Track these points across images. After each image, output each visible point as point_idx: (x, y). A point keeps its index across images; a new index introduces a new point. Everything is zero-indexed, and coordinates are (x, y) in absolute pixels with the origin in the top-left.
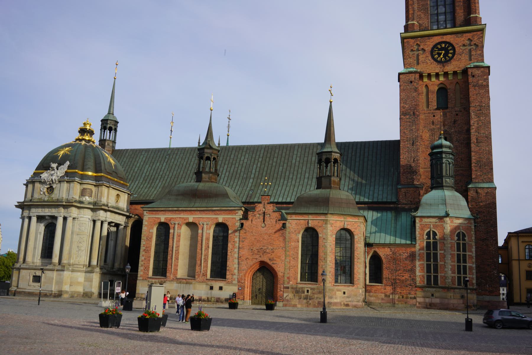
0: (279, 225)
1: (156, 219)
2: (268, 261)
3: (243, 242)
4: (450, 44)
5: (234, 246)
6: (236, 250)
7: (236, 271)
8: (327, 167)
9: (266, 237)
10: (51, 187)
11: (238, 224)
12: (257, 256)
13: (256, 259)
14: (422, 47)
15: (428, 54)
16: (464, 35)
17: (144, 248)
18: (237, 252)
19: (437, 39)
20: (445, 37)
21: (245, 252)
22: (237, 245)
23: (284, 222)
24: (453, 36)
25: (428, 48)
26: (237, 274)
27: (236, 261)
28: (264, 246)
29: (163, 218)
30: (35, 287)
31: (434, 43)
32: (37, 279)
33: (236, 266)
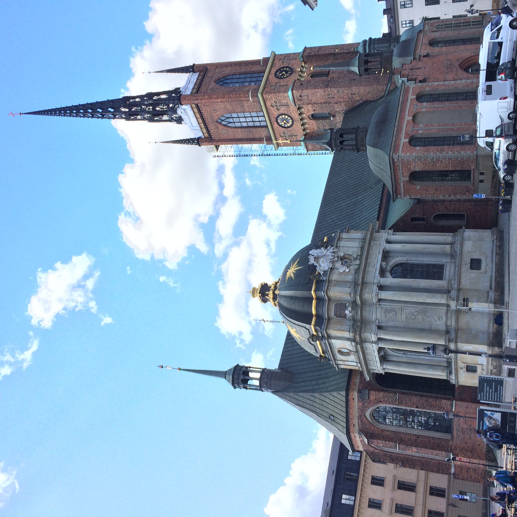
0: (425, 59)
1: (405, 146)
2: (459, 62)
3: (438, 79)
4: (280, 69)
5: (441, 85)
6: (447, 83)
7: (469, 81)
8: (371, 62)
9: (435, 65)
10: (342, 259)
11: (420, 84)
12: (454, 69)
13: (457, 69)
14: (274, 84)
15: (281, 80)
16: (275, 62)
17: (438, 153)
18: (449, 82)
19: (272, 76)
20: (272, 72)
21: (449, 76)
22: (441, 83)
23: (422, 57)
24: (273, 69)
25: (277, 80)
26: (471, 80)
27: (458, 82)
28: (444, 66)
29: (404, 140)
30: (488, 265)
31: (274, 78)
32: (475, 264)
33: (463, 81)
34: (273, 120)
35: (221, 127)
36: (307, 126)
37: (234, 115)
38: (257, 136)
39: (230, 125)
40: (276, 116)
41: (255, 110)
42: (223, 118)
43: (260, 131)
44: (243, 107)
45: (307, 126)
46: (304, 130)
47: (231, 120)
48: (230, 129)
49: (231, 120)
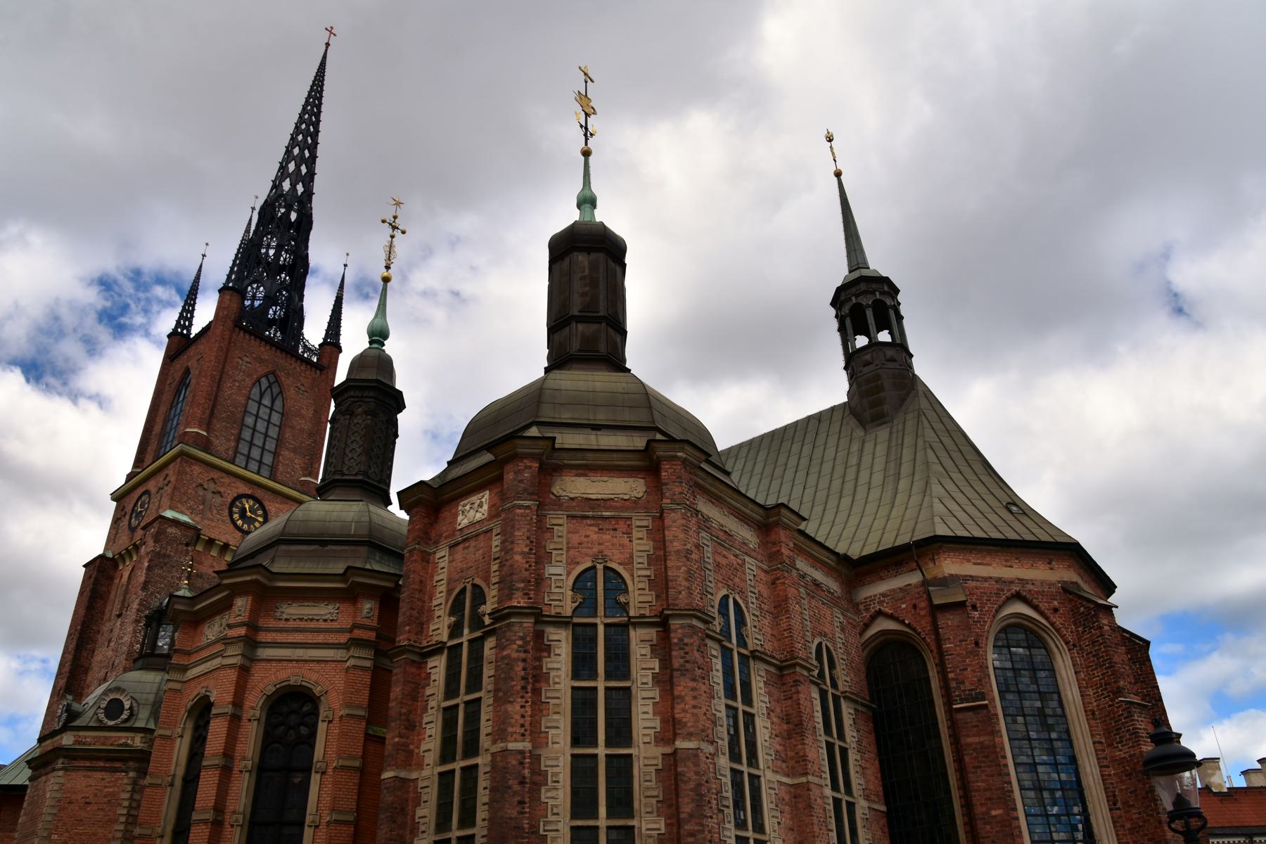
34: (259, 493)
35: (262, 370)
36: (214, 553)
37: (276, 418)
38: (217, 425)
39: (256, 391)
40: (266, 503)
41: (281, 468)
42: (276, 390)
43: (229, 440)
44: (294, 450)
45: (214, 553)
46: (211, 542)
47: (267, 402)
48: (249, 382)
49: (267, 402)
